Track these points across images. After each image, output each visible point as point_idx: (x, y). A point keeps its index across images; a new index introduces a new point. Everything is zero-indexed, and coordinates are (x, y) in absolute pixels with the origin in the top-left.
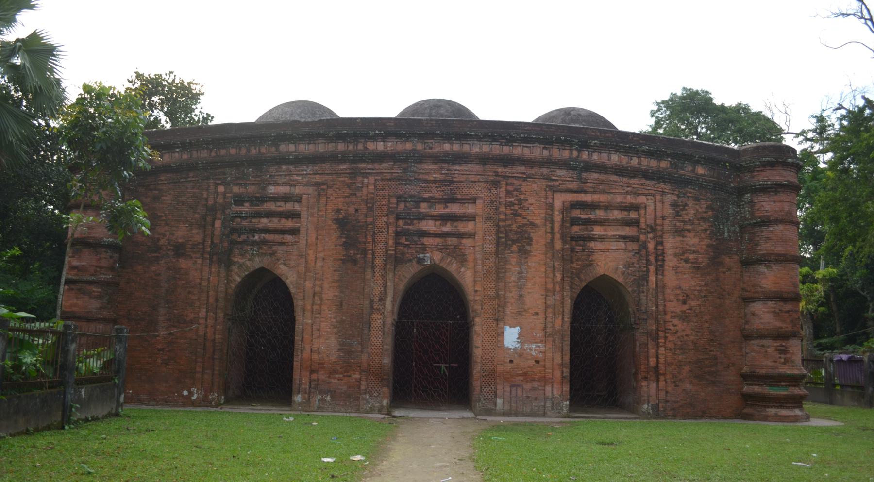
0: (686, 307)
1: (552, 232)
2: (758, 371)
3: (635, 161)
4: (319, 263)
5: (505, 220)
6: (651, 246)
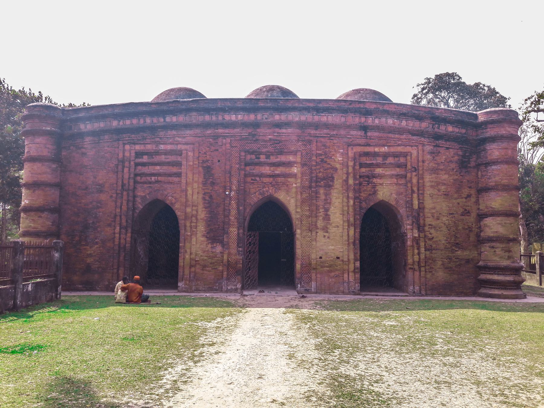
0: (438, 222)
2: (489, 264)
3: (404, 123)
4: (195, 197)
5: (316, 166)
6: (415, 181)
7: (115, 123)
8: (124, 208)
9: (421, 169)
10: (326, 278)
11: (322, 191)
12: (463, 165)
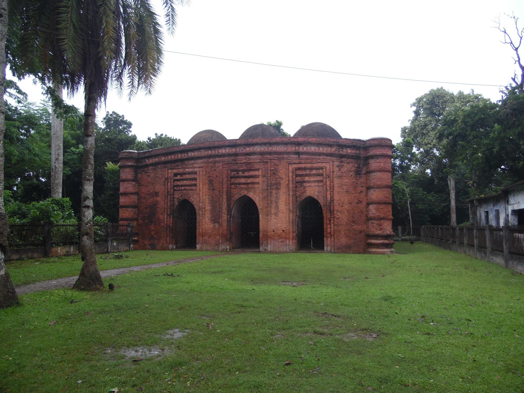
0: (342, 208)
1: (289, 181)
3: (321, 149)
4: (204, 197)
6: (328, 183)
8: (169, 204)
9: (331, 176)
10: (277, 243)
12: (358, 173)
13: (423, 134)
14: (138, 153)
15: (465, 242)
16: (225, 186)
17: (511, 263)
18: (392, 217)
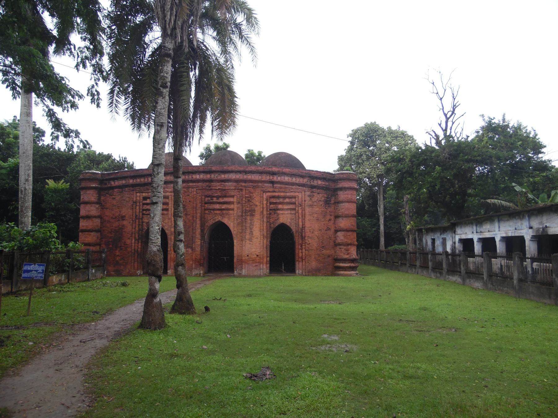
1: (263, 208)
3: (294, 179)
6: (300, 212)
7: (131, 181)
8: (137, 228)
11: (248, 218)
12: (327, 202)
13: (358, 164)
14: (102, 174)
15: (418, 263)
16: (199, 211)
17: (468, 281)
18: (356, 243)
